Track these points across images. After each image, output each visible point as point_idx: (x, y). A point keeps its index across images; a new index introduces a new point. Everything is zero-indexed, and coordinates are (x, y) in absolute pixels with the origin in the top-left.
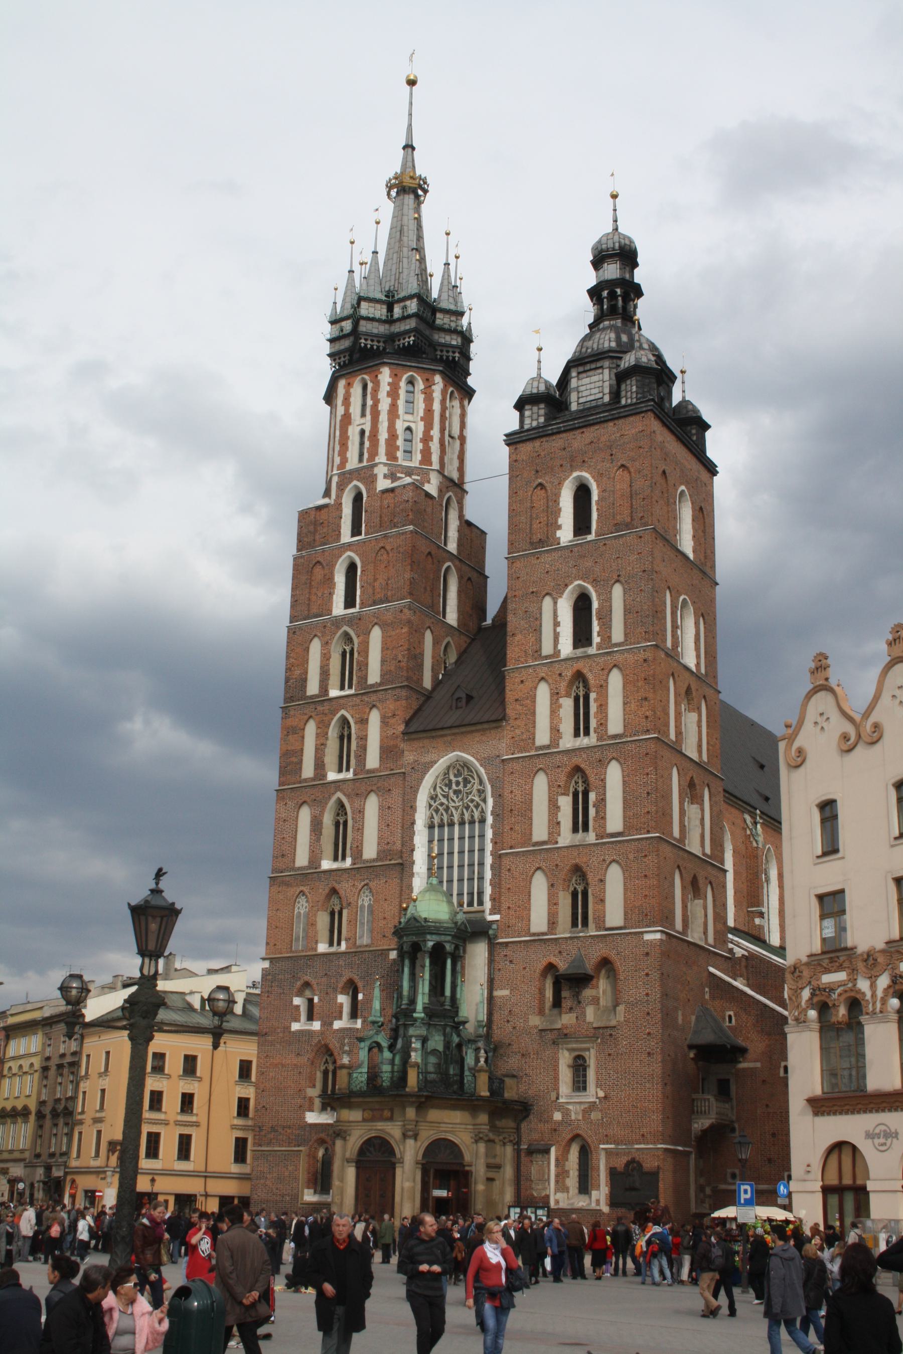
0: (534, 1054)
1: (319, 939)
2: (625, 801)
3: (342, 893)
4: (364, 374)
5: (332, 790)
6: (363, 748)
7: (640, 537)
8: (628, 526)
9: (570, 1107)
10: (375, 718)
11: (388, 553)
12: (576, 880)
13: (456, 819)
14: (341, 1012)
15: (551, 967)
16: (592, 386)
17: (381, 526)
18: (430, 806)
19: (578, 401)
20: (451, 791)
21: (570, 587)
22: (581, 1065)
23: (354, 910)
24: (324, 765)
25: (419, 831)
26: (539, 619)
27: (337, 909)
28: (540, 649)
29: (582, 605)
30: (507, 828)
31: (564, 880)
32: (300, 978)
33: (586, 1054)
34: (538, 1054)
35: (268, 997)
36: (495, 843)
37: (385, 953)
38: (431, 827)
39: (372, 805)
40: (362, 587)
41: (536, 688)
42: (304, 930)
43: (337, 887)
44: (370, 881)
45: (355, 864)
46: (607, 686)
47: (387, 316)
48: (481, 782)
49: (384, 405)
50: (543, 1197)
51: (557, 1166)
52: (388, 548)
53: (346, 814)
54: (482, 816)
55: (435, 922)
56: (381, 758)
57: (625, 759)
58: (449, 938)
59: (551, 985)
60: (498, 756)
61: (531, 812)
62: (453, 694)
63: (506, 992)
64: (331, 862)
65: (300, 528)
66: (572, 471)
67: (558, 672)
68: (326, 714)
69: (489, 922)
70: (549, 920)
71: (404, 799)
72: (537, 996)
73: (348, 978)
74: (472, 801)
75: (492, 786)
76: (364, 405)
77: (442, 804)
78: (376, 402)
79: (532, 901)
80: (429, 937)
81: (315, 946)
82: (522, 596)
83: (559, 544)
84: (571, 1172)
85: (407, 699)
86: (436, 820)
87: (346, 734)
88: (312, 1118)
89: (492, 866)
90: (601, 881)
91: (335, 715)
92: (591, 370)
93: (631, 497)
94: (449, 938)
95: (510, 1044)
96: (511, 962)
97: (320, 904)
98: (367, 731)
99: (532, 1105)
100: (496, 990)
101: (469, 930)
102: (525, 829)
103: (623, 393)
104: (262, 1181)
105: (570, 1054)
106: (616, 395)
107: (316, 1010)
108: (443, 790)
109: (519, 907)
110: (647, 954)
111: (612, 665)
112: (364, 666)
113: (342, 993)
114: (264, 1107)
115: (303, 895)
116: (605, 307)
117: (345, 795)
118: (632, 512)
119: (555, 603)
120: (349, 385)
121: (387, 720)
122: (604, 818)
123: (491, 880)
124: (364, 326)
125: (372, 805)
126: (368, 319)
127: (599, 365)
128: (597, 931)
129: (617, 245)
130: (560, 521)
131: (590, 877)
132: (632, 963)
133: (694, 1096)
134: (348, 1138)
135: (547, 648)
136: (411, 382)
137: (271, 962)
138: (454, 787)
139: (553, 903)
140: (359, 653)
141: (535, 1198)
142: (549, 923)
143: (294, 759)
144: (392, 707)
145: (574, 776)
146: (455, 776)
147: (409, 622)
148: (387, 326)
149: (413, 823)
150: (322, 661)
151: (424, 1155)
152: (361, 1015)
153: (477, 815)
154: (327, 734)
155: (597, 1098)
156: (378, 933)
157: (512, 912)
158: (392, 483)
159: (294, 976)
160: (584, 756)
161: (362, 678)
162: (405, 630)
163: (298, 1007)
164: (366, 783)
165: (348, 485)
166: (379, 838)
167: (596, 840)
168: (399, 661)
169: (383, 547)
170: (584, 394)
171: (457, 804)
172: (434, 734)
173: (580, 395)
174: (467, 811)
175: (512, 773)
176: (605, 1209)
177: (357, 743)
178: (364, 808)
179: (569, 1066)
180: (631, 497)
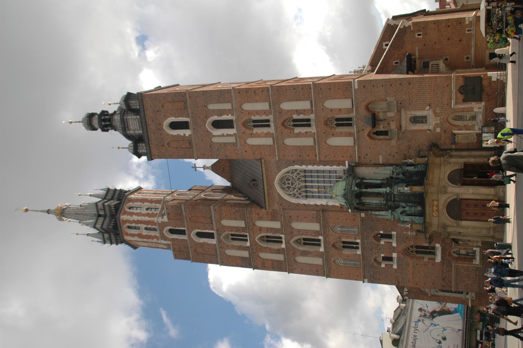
0: (409, 142)
2: (297, 100)
4: (123, 226)
7: (190, 97)
8: (185, 102)
9: (434, 123)
11: (192, 217)
12: (331, 124)
13: (303, 184)
14: (389, 242)
15: (369, 135)
16: (133, 124)
17: (182, 220)
18: (298, 197)
19: (139, 130)
21: (208, 129)
22: (414, 120)
24: (279, 249)
26: (220, 144)
27: (342, 245)
28: (233, 143)
29: (217, 125)
32: (373, 263)
33: (409, 116)
34: (409, 140)
35: (381, 280)
36: (314, 164)
37: (362, 219)
38: (307, 197)
39: (297, 225)
40: (205, 229)
41: (249, 145)
42: (351, 261)
43: (332, 243)
45: (322, 234)
46: (249, 111)
47: (103, 217)
48: (288, 172)
49: (135, 218)
50: (477, 137)
51: (462, 130)
52: (190, 216)
53: (300, 239)
54: (303, 171)
55: (346, 186)
57: (279, 101)
58: (354, 181)
60: (277, 163)
61: (301, 146)
62: (251, 187)
63: (381, 157)
64: (321, 247)
65: (181, 258)
66: (163, 129)
68: (257, 248)
69: (349, 167)
70: (348, 136)
74: (296, 176)
75: (290, 166)
76: (135, 228)
77: (297, 191)
78: (134, 222)
79: (340, 145)
80: (353, 189)
81: (358, 256)
82: (211, 152)
83: (191, 135)
84: (465, 124)
85: (252, 208)
86: (304, 194)
87: (266, 239)
88: (438, 259)
89: (324, 165)
90: (331, 110)
91: (257, 243)
92: (127, 125)
93: (174, 102)
94: (354, 181)
95: (405, 155)
98: (265, 228)
99: (433, 143)
100: (379, 162)
101: (351, 173)
103: (135, 107)
104: (469, 286)
105: (409, 124)
106: (136, 112)
107: (387, 255)
108: (291, 191)
109: (342, 151)
110: (364, 87)
112: (237, 229)
113: (380, 242)
114: (433, 284)
115: (335, 261)
116: (108, 123)
117: (291, 239)
118: (180, 101)
119: (215, 136)
120: (127, 234)
121: (260, 218)
122: (304, 110)
123: (330, 166)
124: (105, 227)
125: (297, 225)
126: (102, 225)
127: (125, 121)
128: (353, 112)
129: (87, 119)
130: (182, 134)
131: (329, 116)
132: (368, 94)
133: (430, 72)
135: (232, 140)
136: (130, 208)
137: (365, 278)
138: (290, 185)
139: (341, 135)
140: (232, 231)
141: (477, 140)
142: (350, 136)
145: (286, 126)
146: (285, 185)
148: (107, 217)
149: (304, 205)
152: (390, 232)
153: (303, 174)
154: (265, 247)
155: (430, 110)
156: (353, 223)
158: (165, 215)
162: (223, 208)
163: (386, 265)
164: (287, 228)
165: (165, 235)
168: (236, 211)
169: (190, 219)
170: (136, 127)
171: (297, 184)
173: (136, 129)
174: (300, 179)
175: (284, 156)
176: (483, 104)
178: (298, 230)
180: (174, 102)
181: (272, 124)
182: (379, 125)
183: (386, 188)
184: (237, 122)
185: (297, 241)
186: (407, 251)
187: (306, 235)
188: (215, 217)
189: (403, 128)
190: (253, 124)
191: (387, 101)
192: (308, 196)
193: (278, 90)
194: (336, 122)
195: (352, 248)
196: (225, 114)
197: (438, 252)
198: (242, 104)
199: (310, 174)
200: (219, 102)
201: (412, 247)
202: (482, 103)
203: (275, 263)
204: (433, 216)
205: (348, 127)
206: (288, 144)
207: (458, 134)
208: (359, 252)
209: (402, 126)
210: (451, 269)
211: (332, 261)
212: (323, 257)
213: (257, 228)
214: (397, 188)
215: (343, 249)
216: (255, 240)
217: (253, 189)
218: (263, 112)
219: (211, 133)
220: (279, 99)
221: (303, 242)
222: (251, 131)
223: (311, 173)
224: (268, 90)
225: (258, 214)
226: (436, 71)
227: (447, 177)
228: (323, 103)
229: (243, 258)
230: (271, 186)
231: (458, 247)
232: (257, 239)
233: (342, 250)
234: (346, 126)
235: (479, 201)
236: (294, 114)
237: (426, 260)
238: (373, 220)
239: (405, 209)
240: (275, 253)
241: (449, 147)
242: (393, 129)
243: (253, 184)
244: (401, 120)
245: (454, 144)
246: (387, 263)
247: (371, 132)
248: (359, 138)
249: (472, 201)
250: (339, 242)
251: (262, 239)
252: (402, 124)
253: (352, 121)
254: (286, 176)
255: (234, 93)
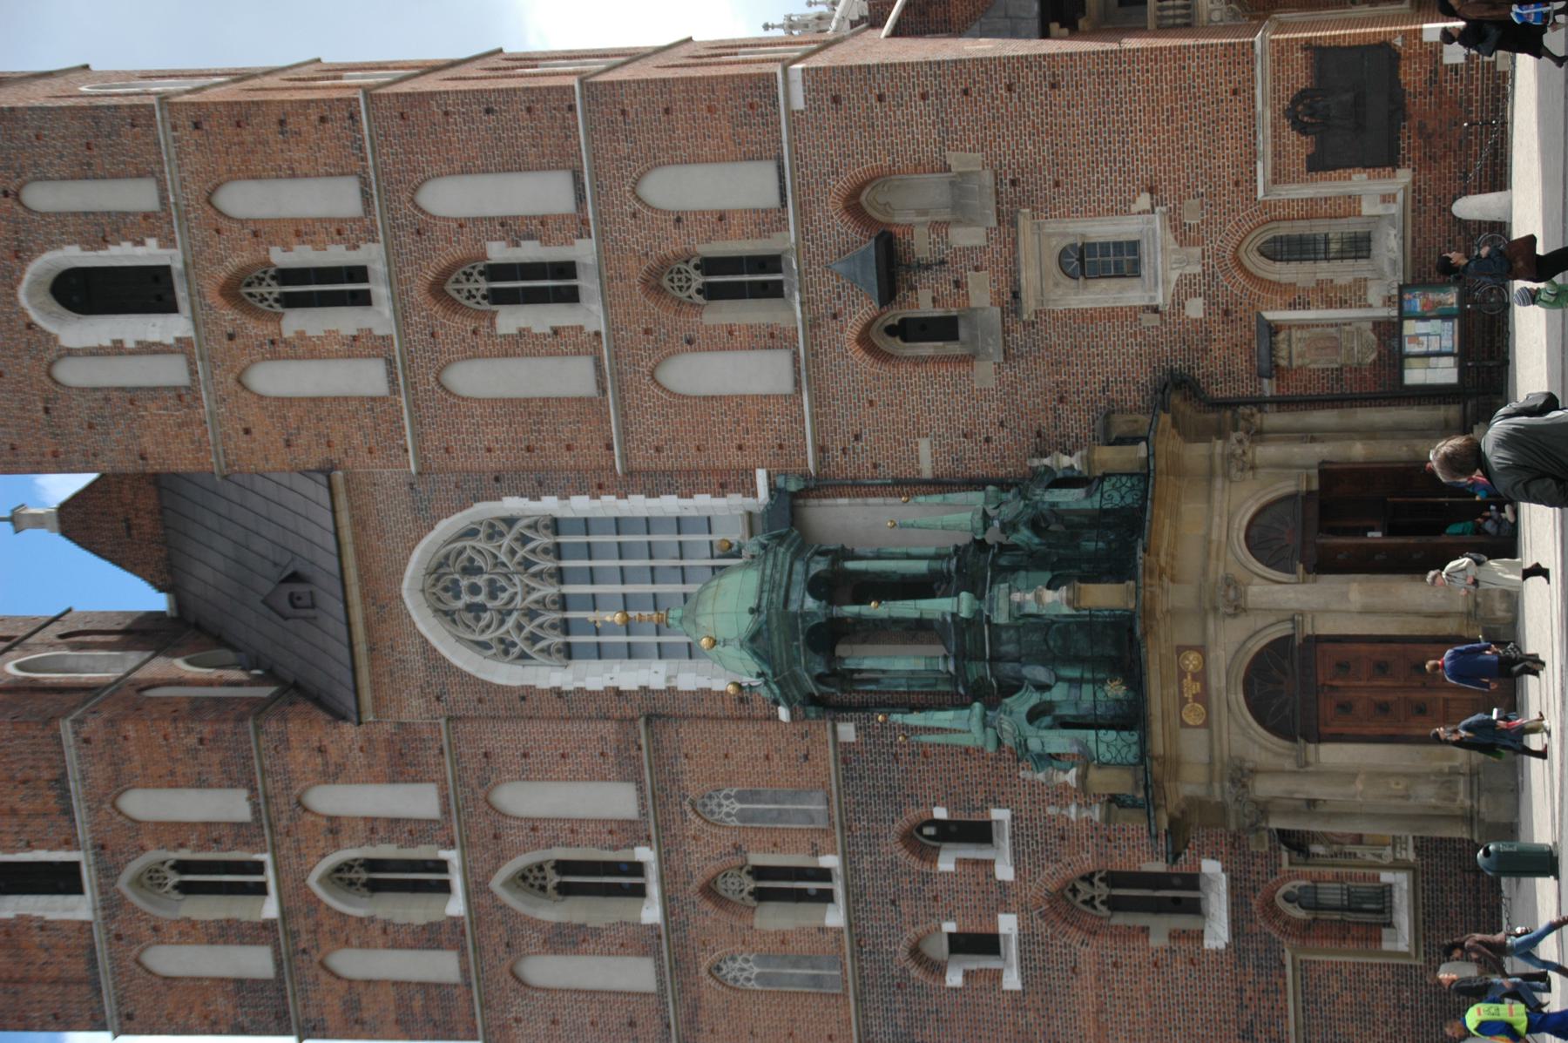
0: (1058, 373)
1: (816, 923)
2: (506, 168)
3: (711, 868)
5: (485, 900)
6: (394, 827)
9: (1174, 276)
10: (329, 799)
12: (681, 288)
13: (550, 590)
14: (977, 862)
15: (865, 341)
18: (523, 656)
20: (489, 605)
21: (34, 316)
22: (1081, 260)
23: (751, 834)
25: (575, 679)
26: (106, 395)
27: (751, 884)
28: (175, 388)
30: (567, 459)
31: (678, 312)
33: (1057, 244)
36: (600, 489)
37: (846, 754)
38: (568, 652)
40: (29, 846)
41: (261, 397)
42: (796, 965)
43: (699, 880)
44: (685, 797)
45: (649, 838)
46: (255, 221)
48: (471, 533)
51: (1306, 305)
53: (540, 868)
54: (546, 527)
55: (762, 591)
56: (416, 780)
57: (414, 171)
58: (799, 567)
59: (907, 344)
60: (411, 485)
61: (532, 400)
63: (924, 447)
64: (647, 902)
67: (225, 341)
69: (771, 496)
70: (766, 347)
71: (507, 719)
72: (931, 369)
73: (900, 846)
74: (513, 552)
75: (477, 500)
77: (520, 627)
79: (726, 391)
81: (832, 935)
84: (1321, 276)
85: (286, 720)
86: (556, 639)
87: (364, 876)
88: (1218, 933)
89: (652, 493)
90: (678, 220)
91: (319, 901)
94: (799, 567)
95: (1039, 434)
96: (857, 438)
97: (737, 924)
98: (354, 819)
100: (919, 472)
101: (784, 530)
102: (569, 414)
105: (1057, 285)
107: (973, 927)
108: (488, 626)
110: (836, 100)
111: (207, 207)
112: (209, 832)
113: (934, 861)
115: (719, 969)
117: (495, 869)
119: (71, 353)
121: (332, 769)
122: (543, 221)
123: (681, 496)
131: (668, 249)
132: (856, 137)
133: (1151, 25)
134: (1249, 765)
135: (172, 372)
138: (481, 598)
139: (728, 340)
140: (182, 846)
142: (772, 348)
143: (417, 1004)
144: (302, 756)
145: (454, 300)
146: (457, 597)
147: (111, 722)
149: (558, 693)
150: (198, 942)
151: (1290, 570)
152: (981, 809)
153: (544, 540)
154: (361, 920)
156: (800, 774)
157: (749, 440)
159: (899, 986)
160: (409, 272)
161: (237, 835)
162: (130, 729)
163: (967, 975)
164: (471, 815)
166: (591, 779)
167: (590, 237)
168: (201, 741)
171: (519, 589)
172: (361, 648)
176: (1404, 176)
177: (382, 840)
178: (527, 819)
179: (1085, 288)
181: (380, 290)
182: (913, 288)
183: (957, 594)
184: (193, 276)
185: (524, 878)
186: (1068, 900)
187: (569, 845)
188: (84, 778)
189: (1029, 304)
190: (277, 290)
191: (948, 169)
192: (575, 651)
193: (402, 114)
194: (702, 279)
195: (801, 896)
196: (125, 239)
197: (1213, 898)
198: (217, 187)
199: (583, 539)
200: (85, 171)
201: (1088, 878)
202: (1400, 172)
203: (412, 999)
204: (1184, 724)
205: (764, 301)
206: (465, 392)
207: (1290, 328)
208: (835, 916)
209: (1023, 295)
210: (1280, 981)
211: (703, 972)
212: (660, 952)
213: (314, 824)
214: (1010, 593)
215: (755, 903)
216: (306, 886)
217: (290, 624)
218: (333, 230)
219: (49, 334)
220: (409, 161)
221: (554, 879)
222: (268, 329)
223: (587, 534)
224: (352, 117)
225: (321, 750)
226: (1178, 21)
227: (1242, 536)
228: (636, 182)
229: (242, 987)
230: (384, 605)
231: (1308, 869)
232: (321, 881)
233: (754, 908)
234: (754, 296)
235: (1395, 646)
236: (492, 239)
237: (1158, 941)
238: (895, 755)
239: (1047, 696)
240: (412, 948)
241: (1246, 389)
242: (983, 309)
243: (291, 596)
244: (1016, 261)
245: (1270, 378)
246: (974, 966)
247: (877, 324)
248: (815, 355)
249: (1364, 648)
250: (736, 872)
251: (347, 876)
252: (1023, 281)
253: (779, 271)
254: (460, 553)
255: (168, 126)
